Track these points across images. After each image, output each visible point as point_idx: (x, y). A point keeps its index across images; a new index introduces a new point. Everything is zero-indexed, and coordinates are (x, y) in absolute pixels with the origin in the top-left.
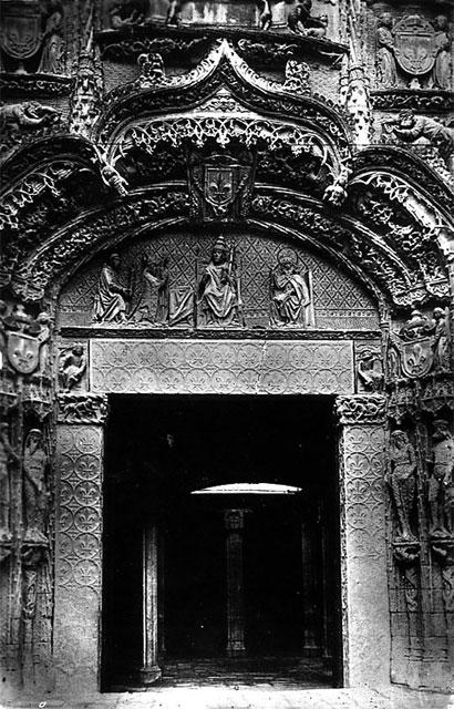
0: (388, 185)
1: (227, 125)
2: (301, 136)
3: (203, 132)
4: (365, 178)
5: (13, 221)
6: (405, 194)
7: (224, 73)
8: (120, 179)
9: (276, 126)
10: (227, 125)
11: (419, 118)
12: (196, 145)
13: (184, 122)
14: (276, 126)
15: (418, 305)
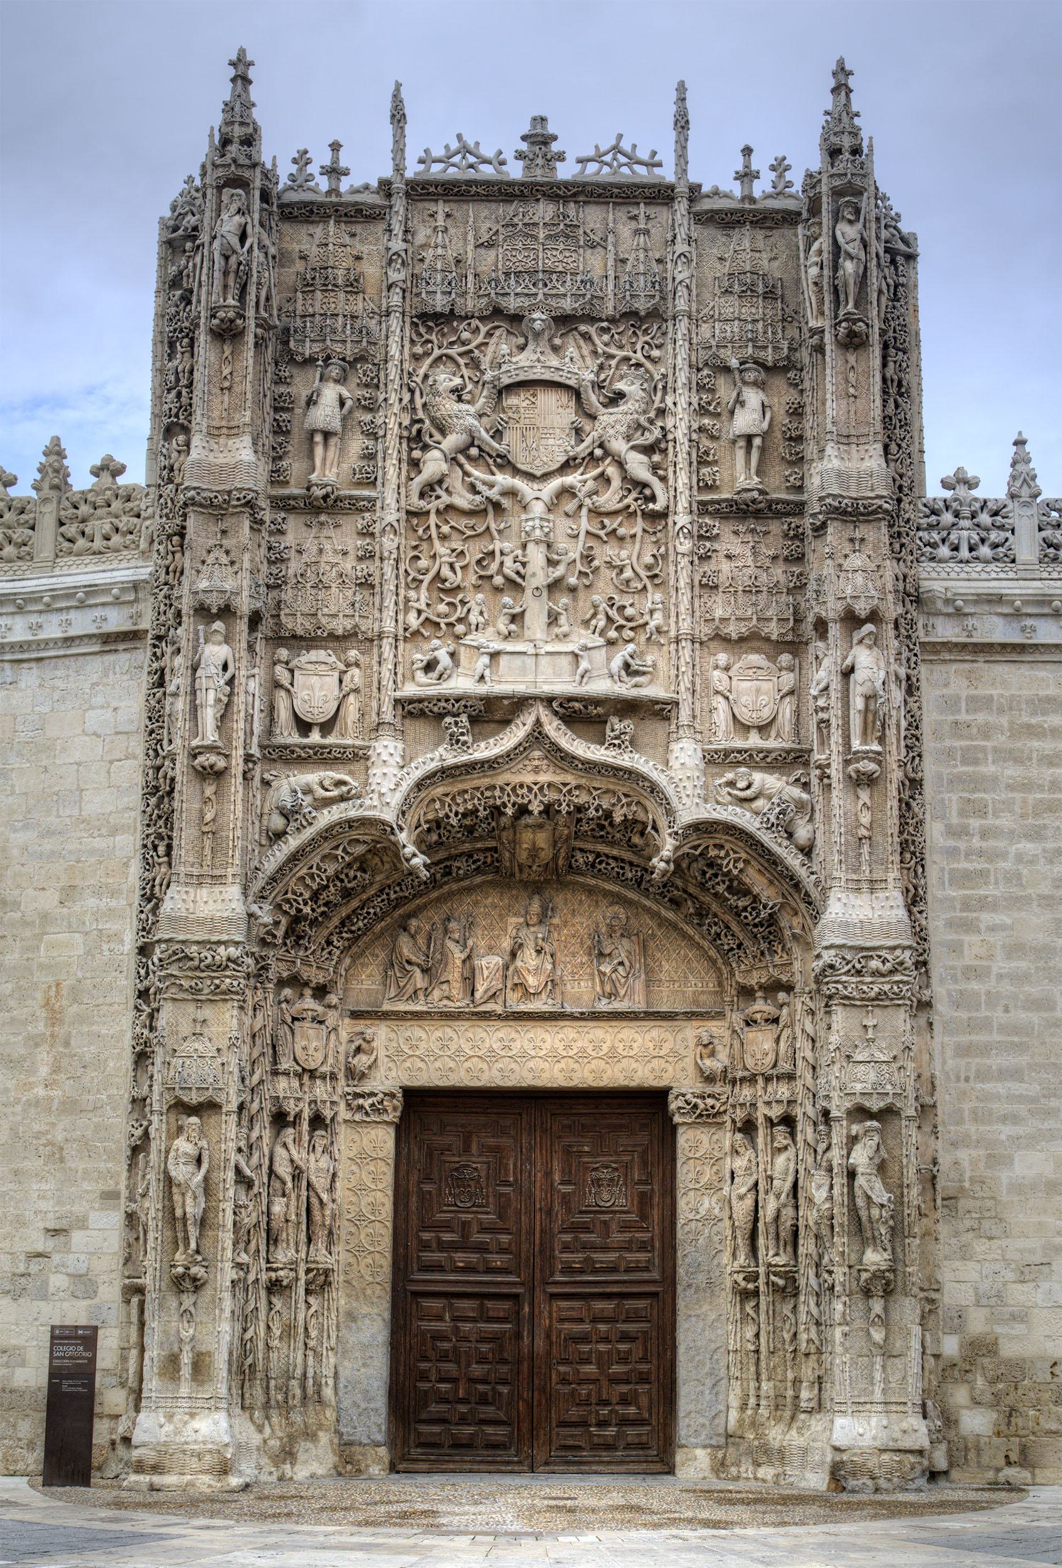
0: (722, 854)
1: (541, 789)
2: (624, 800)
3: (513, 798)
4: (695, 848)
5: (306, 904)
6: (741, 865)
7: (537, 736)
8: (419, 861)
9: (596, 789)
10: (541, 789)
11: (759, 778)
12: (504, 814)
13: (492, 788)
14: (596, 789)
15: (761, 987)
